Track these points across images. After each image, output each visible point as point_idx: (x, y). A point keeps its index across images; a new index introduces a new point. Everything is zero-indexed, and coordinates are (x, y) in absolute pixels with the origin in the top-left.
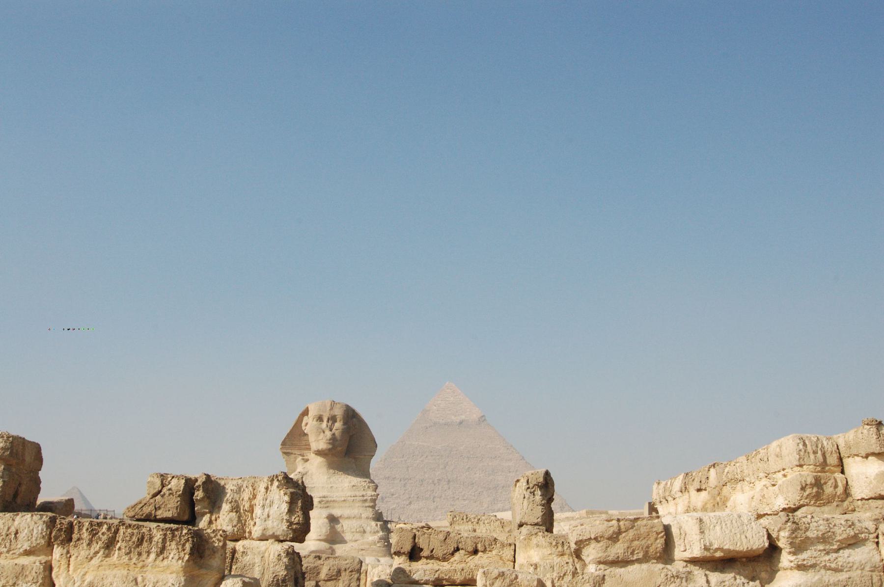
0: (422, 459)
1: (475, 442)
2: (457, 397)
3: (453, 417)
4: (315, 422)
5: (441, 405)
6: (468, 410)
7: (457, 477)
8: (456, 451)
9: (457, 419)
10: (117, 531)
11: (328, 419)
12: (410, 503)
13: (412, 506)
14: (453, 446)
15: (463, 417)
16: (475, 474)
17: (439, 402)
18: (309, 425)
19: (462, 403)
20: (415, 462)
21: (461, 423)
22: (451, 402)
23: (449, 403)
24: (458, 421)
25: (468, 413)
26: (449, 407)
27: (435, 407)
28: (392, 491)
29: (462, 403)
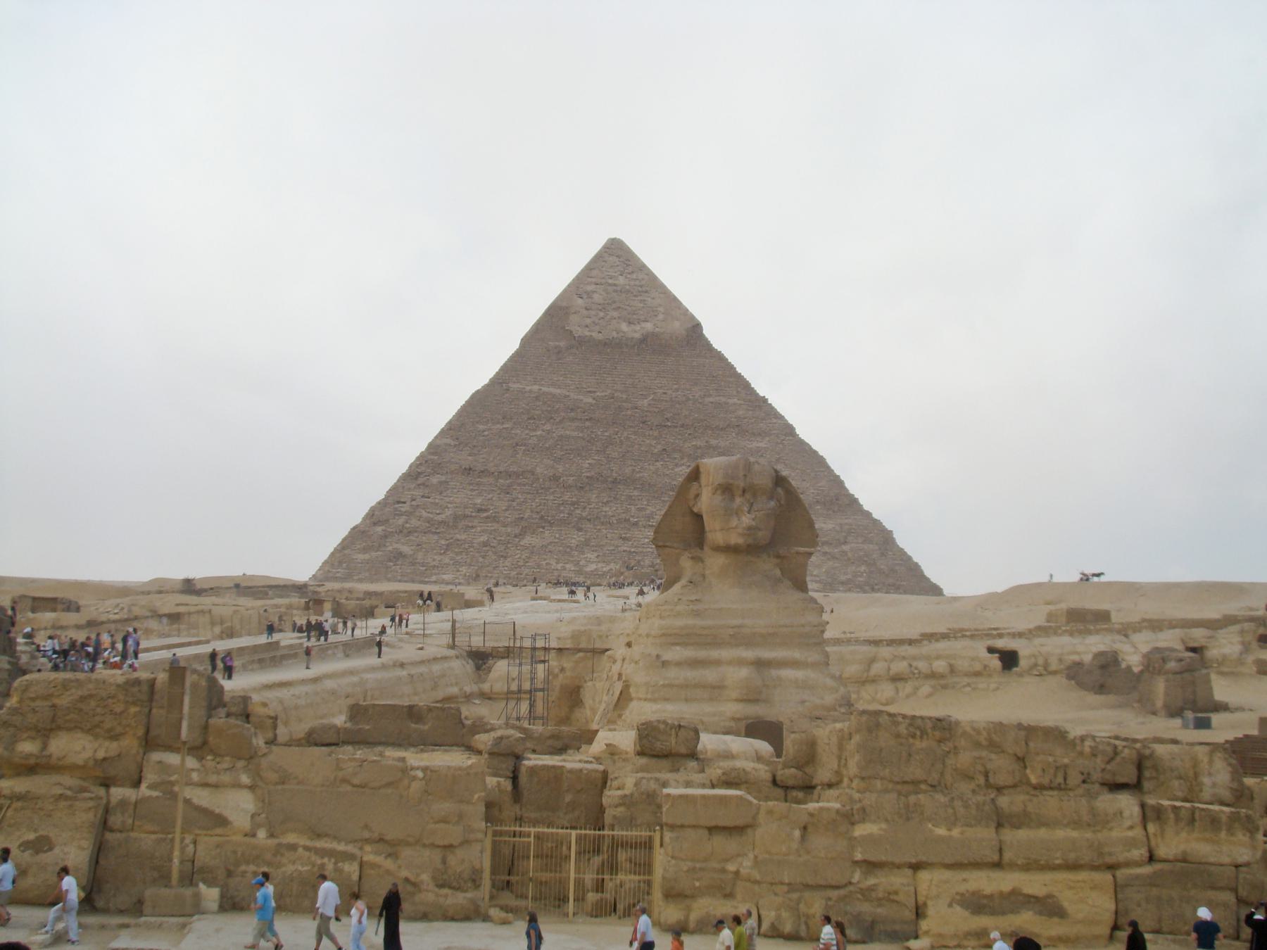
0: (548, 427)
1: (677, 390)
2: (634, 276)
3: (624, 327)
4: (718, 498)
5: (596, 296)
6: (661, 309)
7: (634, 470)
8: (632, 408)
9: (634, 332)
10: (1193, 814)
11: (744, 491)
12: (521, 535)
13: (528, 540)
14: (624, 396)
15: (649, 326)
16: (676, 465)
17: (590, 288)
18: (707, 501)
19: (646, 292)
20: (534, 434)
21: (644, 339)
22: (619, 288)
23: (615, 291)
24: (637, 336)
25: (661, 317)
26: (614, 302)
27: (580, 301)
28: (479, 501)
29: (646, 292)
